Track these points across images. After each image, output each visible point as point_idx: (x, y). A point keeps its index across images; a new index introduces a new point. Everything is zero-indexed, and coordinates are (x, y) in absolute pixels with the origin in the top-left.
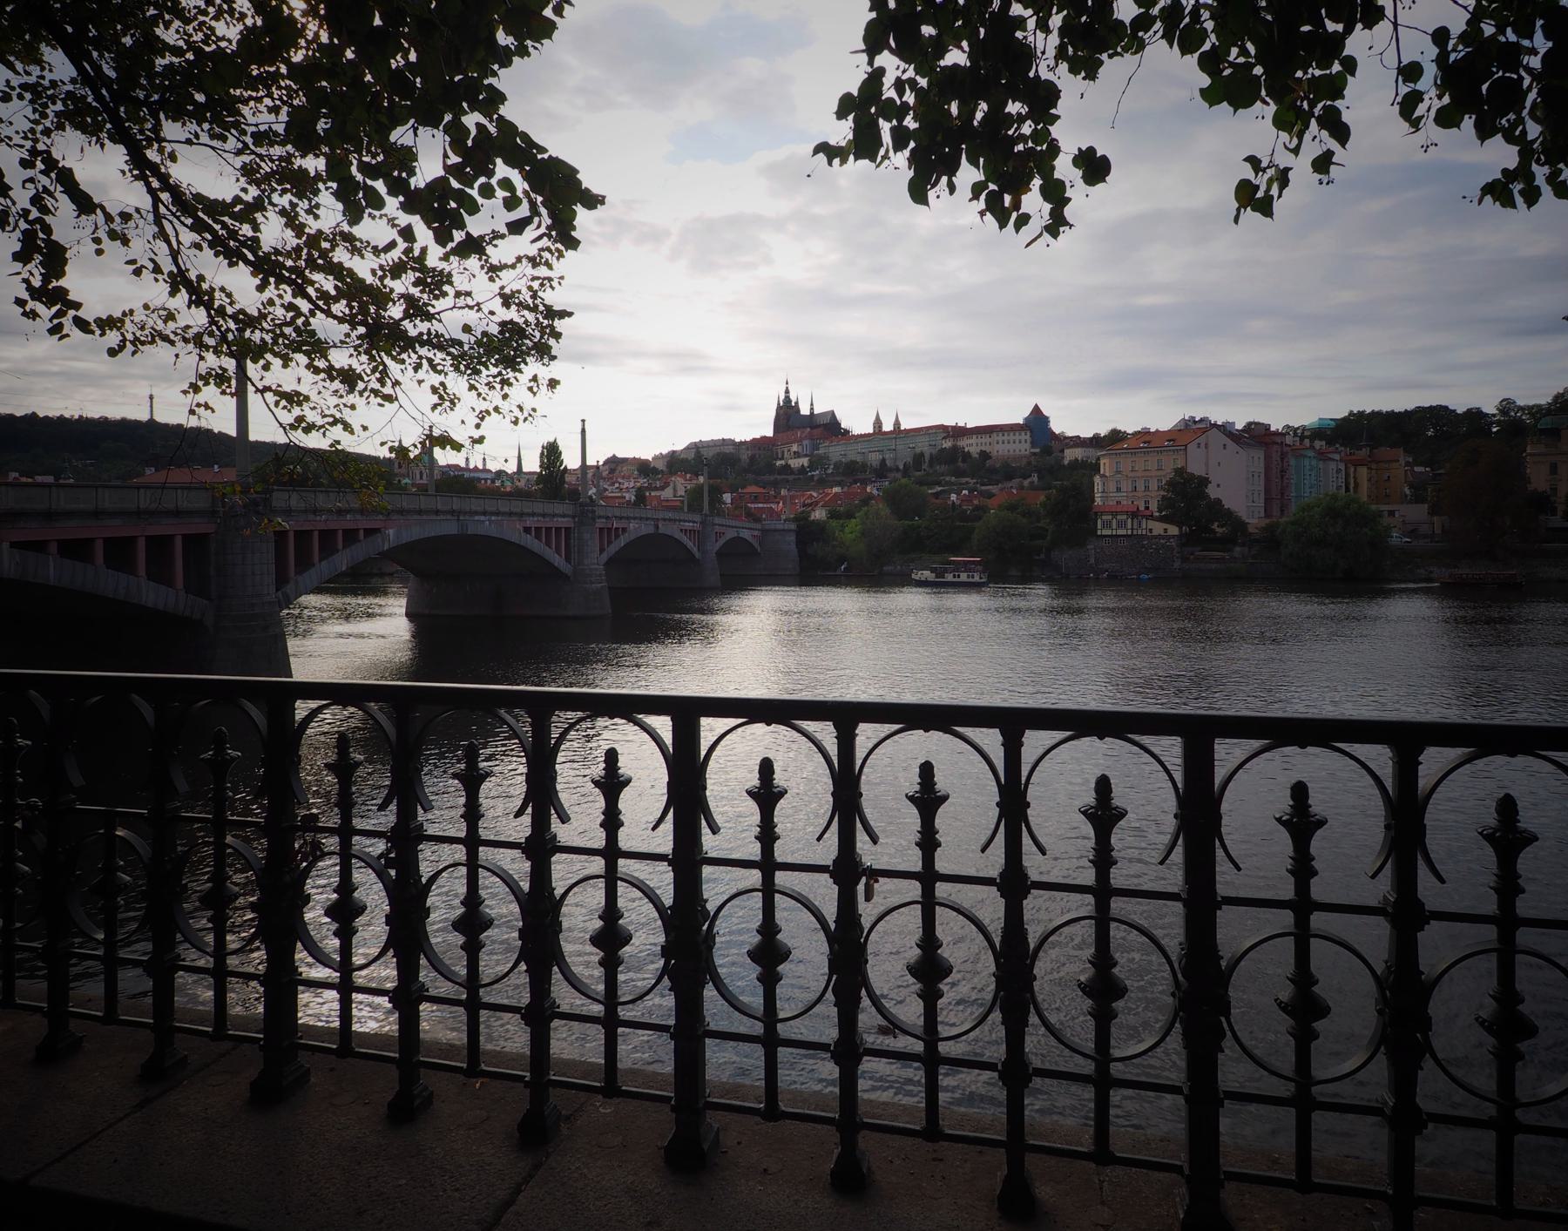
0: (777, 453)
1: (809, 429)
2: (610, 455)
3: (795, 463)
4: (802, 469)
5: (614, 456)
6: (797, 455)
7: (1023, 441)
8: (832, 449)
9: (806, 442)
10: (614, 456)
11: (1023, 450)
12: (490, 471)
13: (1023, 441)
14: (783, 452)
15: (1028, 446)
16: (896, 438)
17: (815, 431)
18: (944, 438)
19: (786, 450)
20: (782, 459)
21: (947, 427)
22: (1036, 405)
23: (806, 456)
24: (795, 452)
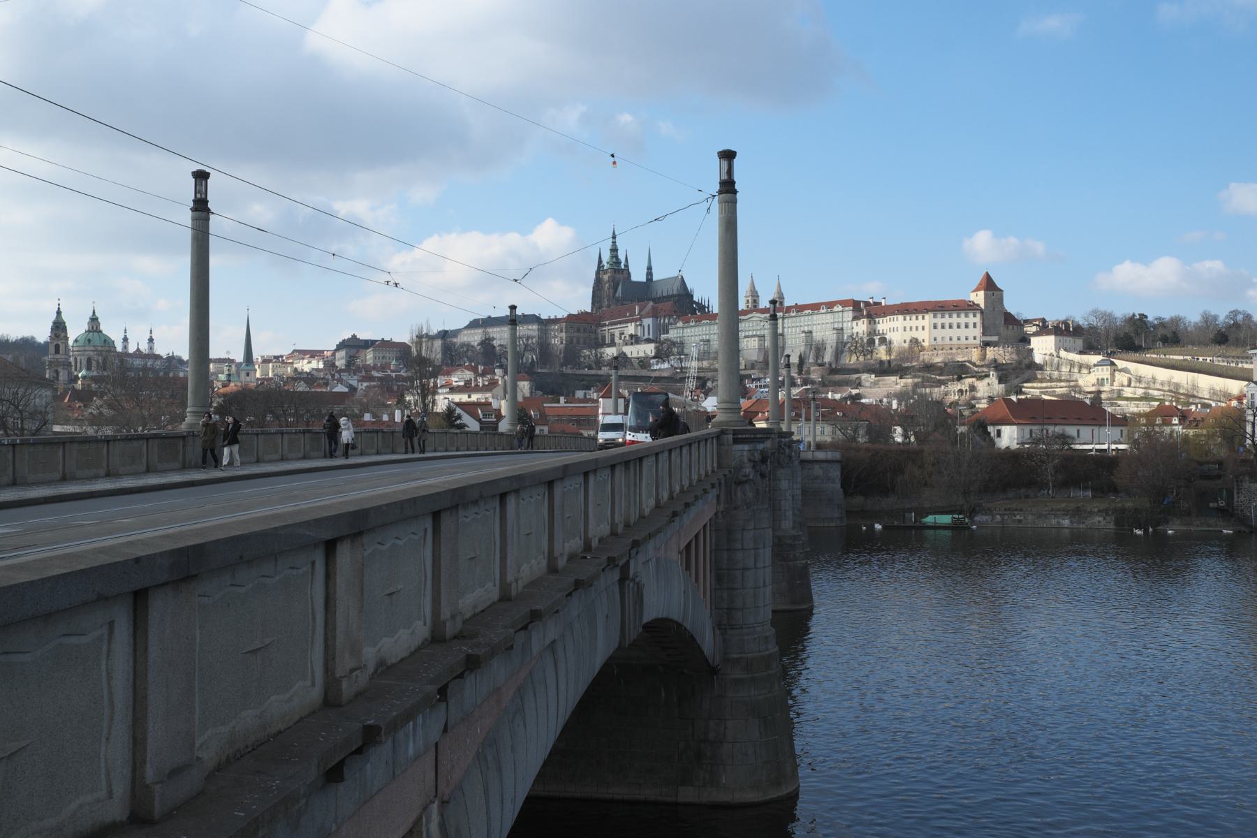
0: (604, 338)
1: (651, 303)
2: (348, 336)
3: (633, 351)
4: (644, 362)
5: (354, 336)
6: (635, 340)
7: (971, 325)
8: (688, 332)
9: (648, 321)
10: (354, 336)
11: (971, 339)
12: (158, 357)
13: (971, 325)
14: (613, 335)
15: (978, 332)
17: (660, 306)
18: (855, 318)
19: (617, 333)
20: (612, 344)
22: (987, 274)
23: (648, 341)
24: (631, 336)
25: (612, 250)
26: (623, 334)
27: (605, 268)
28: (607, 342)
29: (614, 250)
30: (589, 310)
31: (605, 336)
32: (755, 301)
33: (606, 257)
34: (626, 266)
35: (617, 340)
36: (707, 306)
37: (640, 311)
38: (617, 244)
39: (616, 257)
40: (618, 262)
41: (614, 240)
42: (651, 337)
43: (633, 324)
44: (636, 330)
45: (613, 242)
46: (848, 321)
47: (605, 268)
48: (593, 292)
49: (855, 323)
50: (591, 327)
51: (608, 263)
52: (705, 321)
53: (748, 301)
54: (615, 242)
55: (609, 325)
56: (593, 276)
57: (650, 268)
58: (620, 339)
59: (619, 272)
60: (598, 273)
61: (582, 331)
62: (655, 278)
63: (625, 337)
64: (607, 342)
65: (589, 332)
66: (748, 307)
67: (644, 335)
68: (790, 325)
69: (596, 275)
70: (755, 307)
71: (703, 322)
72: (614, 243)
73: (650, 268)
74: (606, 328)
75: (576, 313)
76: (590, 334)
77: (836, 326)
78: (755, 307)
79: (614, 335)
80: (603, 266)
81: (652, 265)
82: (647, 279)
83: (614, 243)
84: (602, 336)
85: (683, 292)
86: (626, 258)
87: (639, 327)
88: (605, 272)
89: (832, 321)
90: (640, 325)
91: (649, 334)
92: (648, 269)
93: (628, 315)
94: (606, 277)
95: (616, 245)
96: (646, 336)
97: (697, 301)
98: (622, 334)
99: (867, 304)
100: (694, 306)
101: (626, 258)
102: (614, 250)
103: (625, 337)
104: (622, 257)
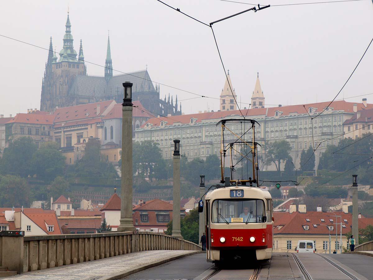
0: (58, 140)
14: (69, 139)
16: (266, 122)
21: (352, 105)
25: (65, 41)
26: (82, 136)
27: (58, 61)
28: (62, 146)
29: (68, 41)
30: (39, 109)
31: (60, 139)
32: (232, 101)
33: (59, 48)
34: (81, 59)
35: (74, 141)
36: (174, 105)
37: (102, 111)
38: (71, 33)
39: (71, 48)
40: (73, 55)
41: (68, 29)
42: (114, 140)
43: (94, 126)
44: (97, 133)
45: (67, 32)
46: (340, 126)
47: (58, 61)
48: (43, 87)
49: (346, 129)
50: (44, 128)
51: (61, 55)
52: (177, 124)
53: (224, 101)
54: (70, 32)
55: (64, 127)
56: (43, 70)
57: (109, 62)
58: (79, 142)
59: (74, 66)
60: (49, 66)
61: (34, 132)
62: (115, 73)
63: (84, 140)
64: (62, 146)
65: (42, 134)
66: (224, 108)
67: (106, 139)
68: (273, 129)
69: (47, 68)
70: (232, 107)
71: (174, 124)
72: (68, 32)
73: (109, 62)
74: (62, 130)
75: (26, 112)
76: (44, 137)
77: (325, 130)
78: (232, 107)
79: (71, 138)
80: (56, 59)
81: (112, 58)
82: (106, 74)
83: (68, 32)
84: (57, 139)
85: (146, 89)
86: (81, 51)
87: (100, 130)
88: (59, 65)
89: (320, 125)
90: (102, 127)
91: (112, 138)
92: (107, 63)
93: (87, 115)
94: (59, 71)
95: (70, 35)
96: (109, 140)
97: (163, 100)
98: (80, 136)
99: (358, 105)
100: (160, 105)
101: (81, 51)
102: (68, 41)
103: (84, 140)
104: (76, 49)
